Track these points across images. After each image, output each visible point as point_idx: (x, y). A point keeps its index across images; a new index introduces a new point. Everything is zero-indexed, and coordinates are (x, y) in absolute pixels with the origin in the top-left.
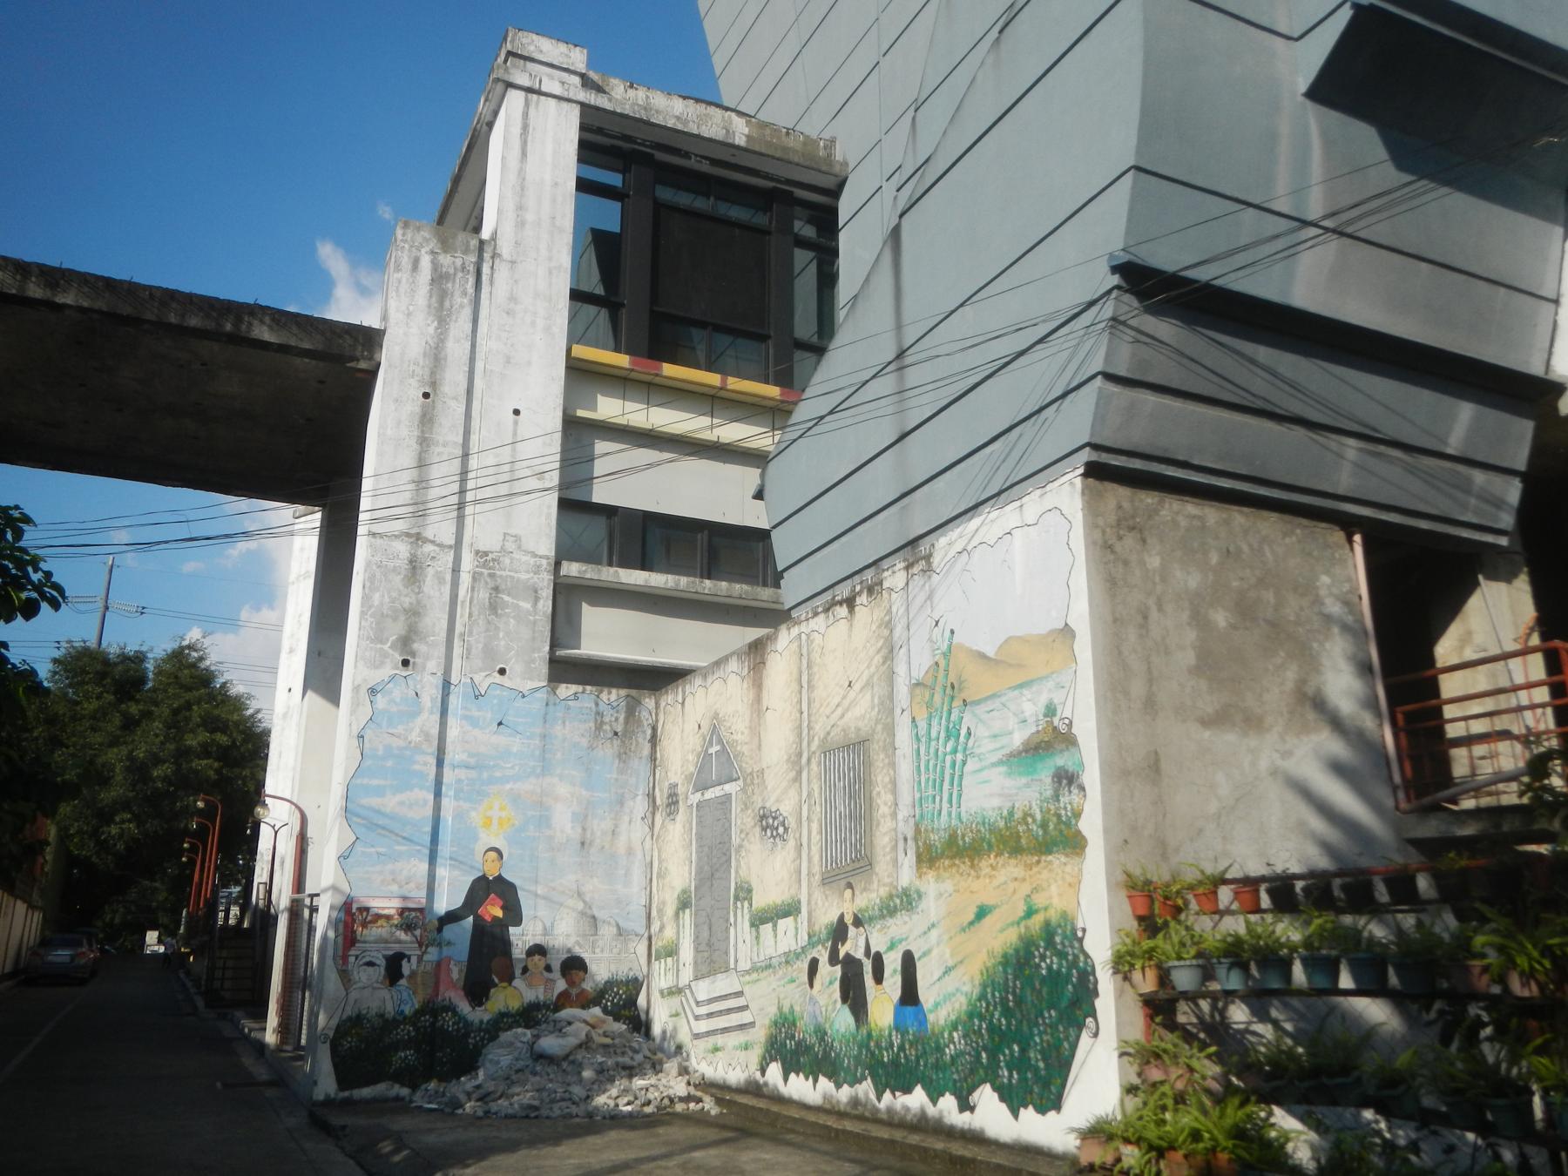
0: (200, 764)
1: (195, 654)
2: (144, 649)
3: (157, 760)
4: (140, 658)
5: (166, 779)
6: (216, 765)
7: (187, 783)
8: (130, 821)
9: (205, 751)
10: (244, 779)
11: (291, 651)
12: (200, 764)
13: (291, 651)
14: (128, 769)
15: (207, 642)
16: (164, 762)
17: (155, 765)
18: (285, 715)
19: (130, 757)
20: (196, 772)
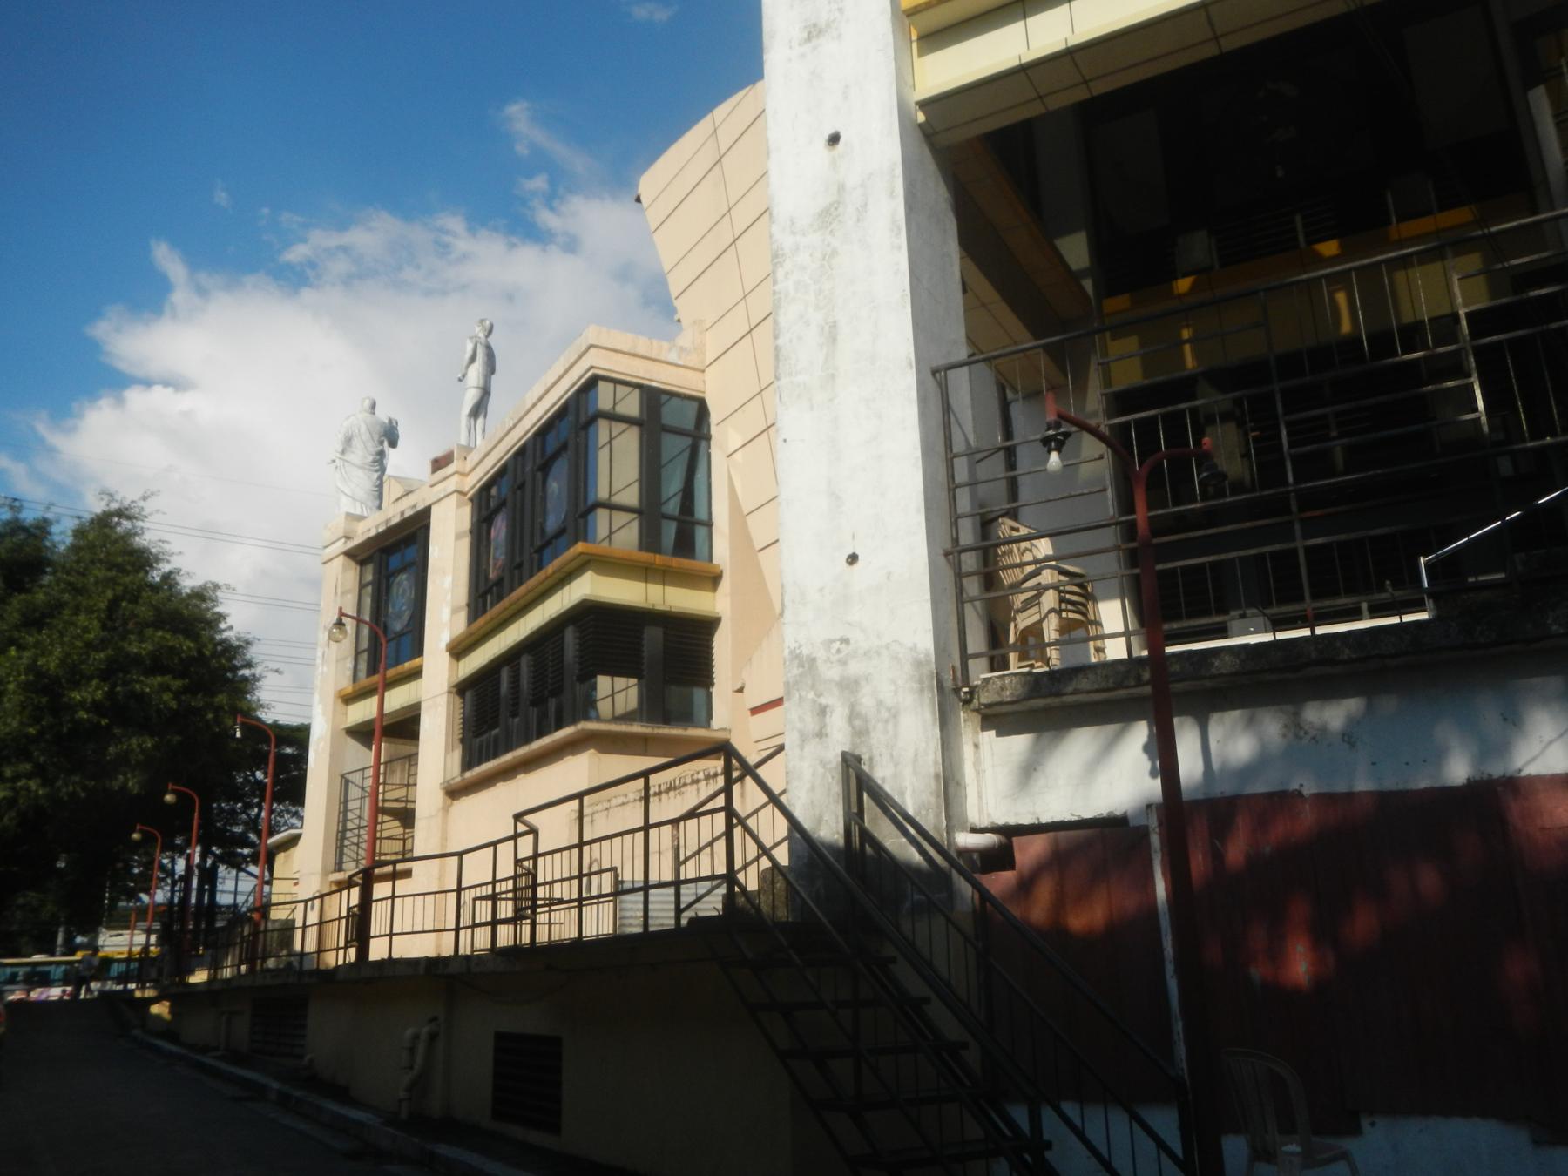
0: (149, 684)
1: (126, 524)
2: (49, 516)
3: (76, 677)
4: (43, 527)
5: (96, 707)
6: (177, 684)
7: (126, 712)
8: (29, 776)
9: (157, 665)
10: (218, 709)
11: (813, 33)
12: (149, 684)
13: (813, 33)
14: (26, 687)
15: (149, 506)
16: (91, 678)
17: (76, 685)
18: (828, 216)
19: (32, 668)
20: (141, 698)
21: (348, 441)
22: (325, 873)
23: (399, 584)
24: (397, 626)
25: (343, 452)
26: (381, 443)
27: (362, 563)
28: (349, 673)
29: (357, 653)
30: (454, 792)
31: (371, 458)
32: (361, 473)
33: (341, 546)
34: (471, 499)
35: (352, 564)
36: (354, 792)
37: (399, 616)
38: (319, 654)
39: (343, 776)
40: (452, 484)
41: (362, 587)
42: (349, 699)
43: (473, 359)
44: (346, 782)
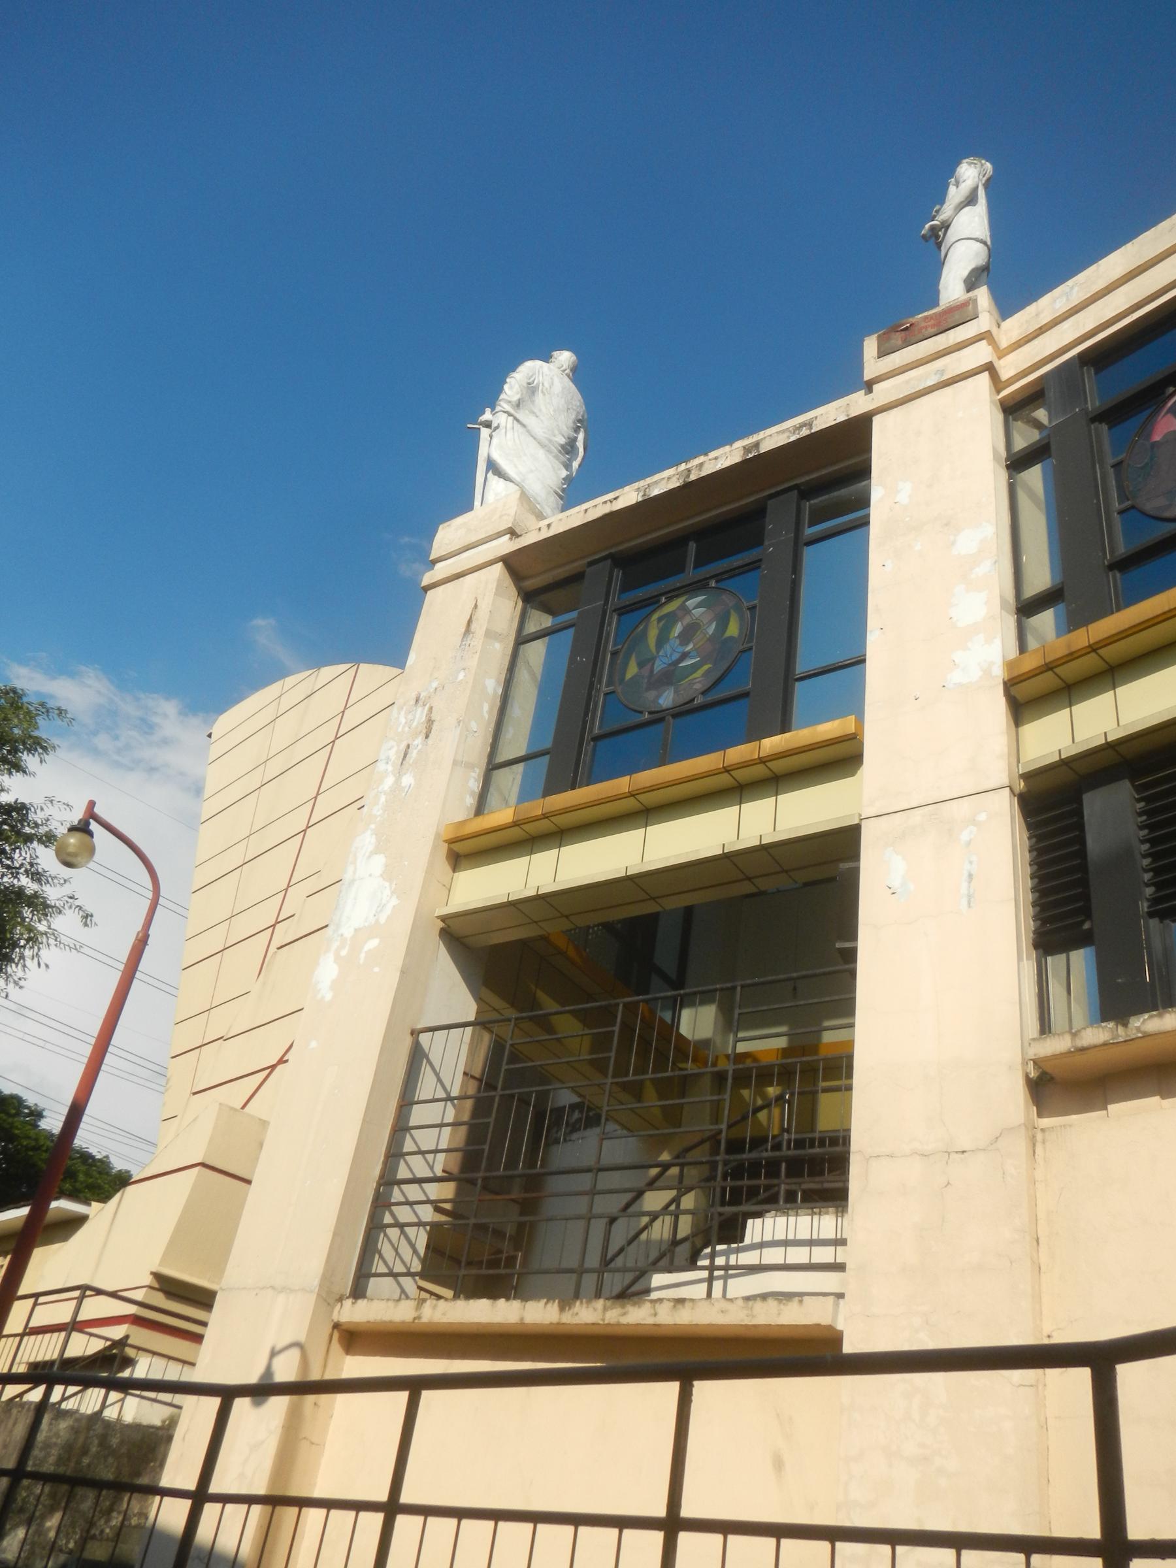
21: (531, 389)
22: (328, 1297)
23: (671, 619)
24: (667, 699)
25: (518, 405)
26: (577, 430)
27: (531, 597)
28: (470, 801)
29: (493, 766)
30: (1059, 1087)
31: (563, 441)
32: (541, 454)
33: (506, 545)
34: (1014, 409)
35: (513, 591)
36: (427, 1087)
37: (668, 677)
38: (392, 752)
39: (415, 1033)
40: (981, 354)
41: (522, 640)
42: (465, 851)
43: (971, 200)
44: (417, 1056)
